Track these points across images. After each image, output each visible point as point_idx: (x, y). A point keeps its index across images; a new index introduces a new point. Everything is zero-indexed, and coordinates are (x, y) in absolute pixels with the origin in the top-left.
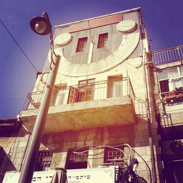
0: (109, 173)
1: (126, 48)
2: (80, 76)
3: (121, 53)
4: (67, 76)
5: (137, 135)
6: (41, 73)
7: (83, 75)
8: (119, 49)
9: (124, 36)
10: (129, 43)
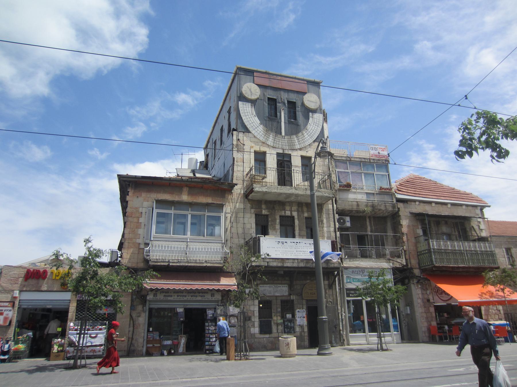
0: (328, 243)
2: (277, 147)
7: (280, 146)
9: (311, 114)
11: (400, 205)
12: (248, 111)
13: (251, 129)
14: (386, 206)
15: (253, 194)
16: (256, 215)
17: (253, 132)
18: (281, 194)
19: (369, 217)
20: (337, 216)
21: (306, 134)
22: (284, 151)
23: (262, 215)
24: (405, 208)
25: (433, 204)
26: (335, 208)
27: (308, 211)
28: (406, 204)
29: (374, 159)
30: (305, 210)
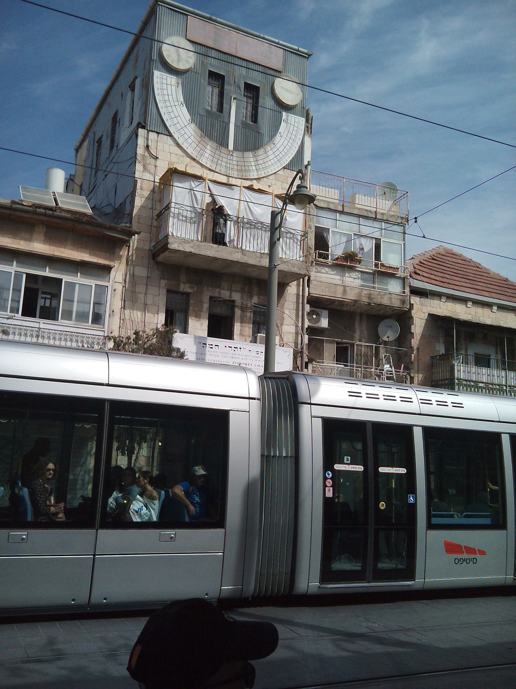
1: (285, 144)
3: (277, 153)
4: (194, 159)
5: (287, 300)
6: (143, 127)
8: (276, 142)
10: (290, 134)
11: (415, 300)
12: (170, 93)
13: (172, 130)
14: (391, 298)
15: (166, 254)
16: (168, 291)
17: (176, 136)
18: (215, 259)
19: (361, 314)
20: (307, 308)
21: (270, 152)
22: (228, 180)
23: (178, 293)
24: (422, 305)
25: (470, 304)
26: (306, 294)
27: (259, 294)
28: (424, 300)
29: (383, 214)
30: (255, 293)
